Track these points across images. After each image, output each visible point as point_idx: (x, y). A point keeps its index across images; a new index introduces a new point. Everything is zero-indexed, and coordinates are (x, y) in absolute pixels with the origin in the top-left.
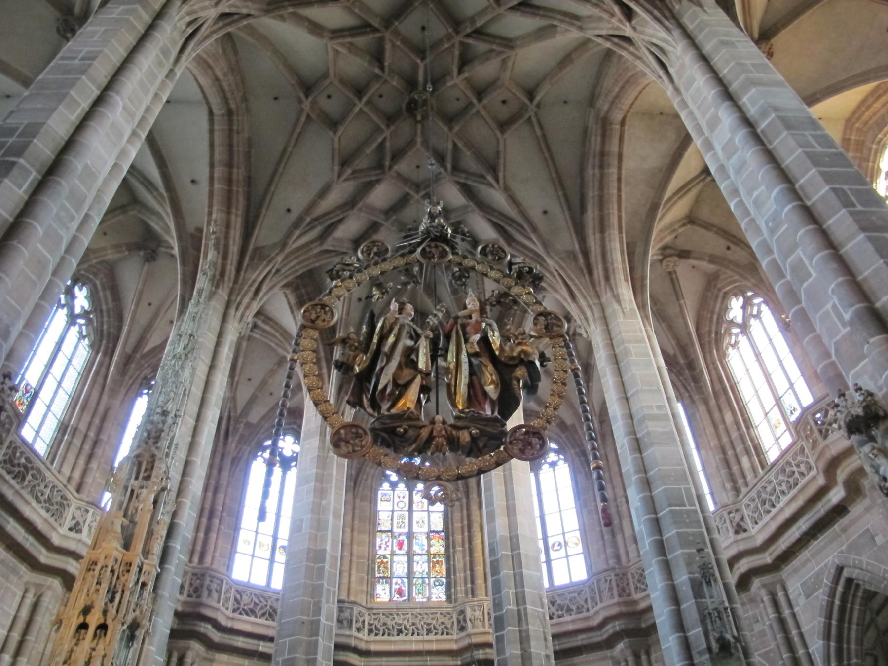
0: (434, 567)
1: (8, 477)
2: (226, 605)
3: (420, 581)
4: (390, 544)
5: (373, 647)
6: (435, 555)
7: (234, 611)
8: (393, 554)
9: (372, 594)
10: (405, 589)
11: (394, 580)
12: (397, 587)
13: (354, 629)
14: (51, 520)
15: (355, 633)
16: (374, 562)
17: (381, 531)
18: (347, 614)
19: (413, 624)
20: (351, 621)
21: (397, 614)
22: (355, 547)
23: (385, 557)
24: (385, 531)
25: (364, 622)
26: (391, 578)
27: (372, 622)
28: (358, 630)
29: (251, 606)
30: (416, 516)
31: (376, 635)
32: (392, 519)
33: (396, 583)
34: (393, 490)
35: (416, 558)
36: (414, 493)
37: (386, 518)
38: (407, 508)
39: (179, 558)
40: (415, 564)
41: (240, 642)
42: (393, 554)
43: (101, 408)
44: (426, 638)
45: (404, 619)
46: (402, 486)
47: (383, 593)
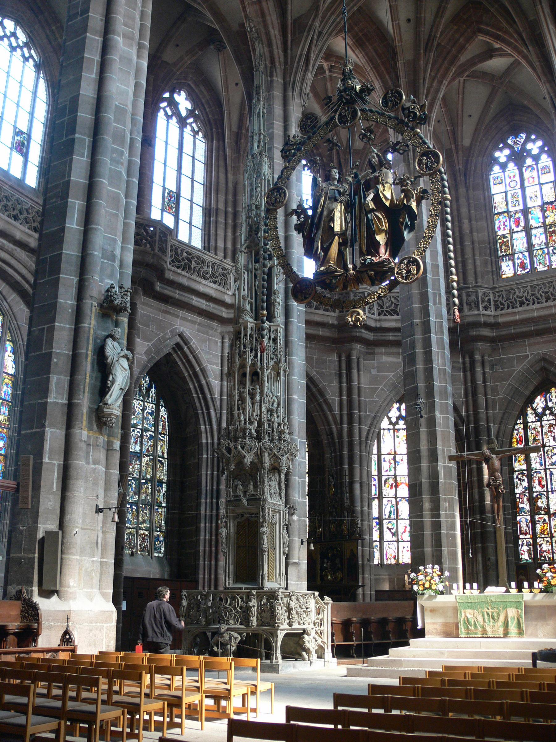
0: (551, 236)
1: (179, 271)
2: (372, 311)
3: (540, 252)
4: (507, 223)
5: (501, 320)
6: (550, 226)
7: (379, 314)
8: (512, 232)
9: (498, 272)
10: (527, 261)
11: (516, 256)
12: (519, 261)
13: (481, 308)
14: (220, 288)
15: (483, 312)
16: (495, 243)
17: (498, 214)
18: (473, 297)
19: (533, 295)
20: (478, 302)
21: (518, 288)
22: (475, 234)
23: (504, 236)
24: (501, 213)
25: (490, 299)
26: (513, 254)
27: (496, 299)
28: (486, 308)
29: (392, 307)
30: (529, 192)
31: (502, 309)
32: (506, 200)
33: (518, 258)
34: (504, 172)
35: (534, 232)
36: (524, 169)
37: (501, 200)
38: (519, 186)
39: (298, 310)
40: (533, 237)
41: (390, 337)
42: (512, 232)
43: (230, 185)
44: (545, 304)
45: (524, 292)
46: (511, 165)
47: (507, 269)
